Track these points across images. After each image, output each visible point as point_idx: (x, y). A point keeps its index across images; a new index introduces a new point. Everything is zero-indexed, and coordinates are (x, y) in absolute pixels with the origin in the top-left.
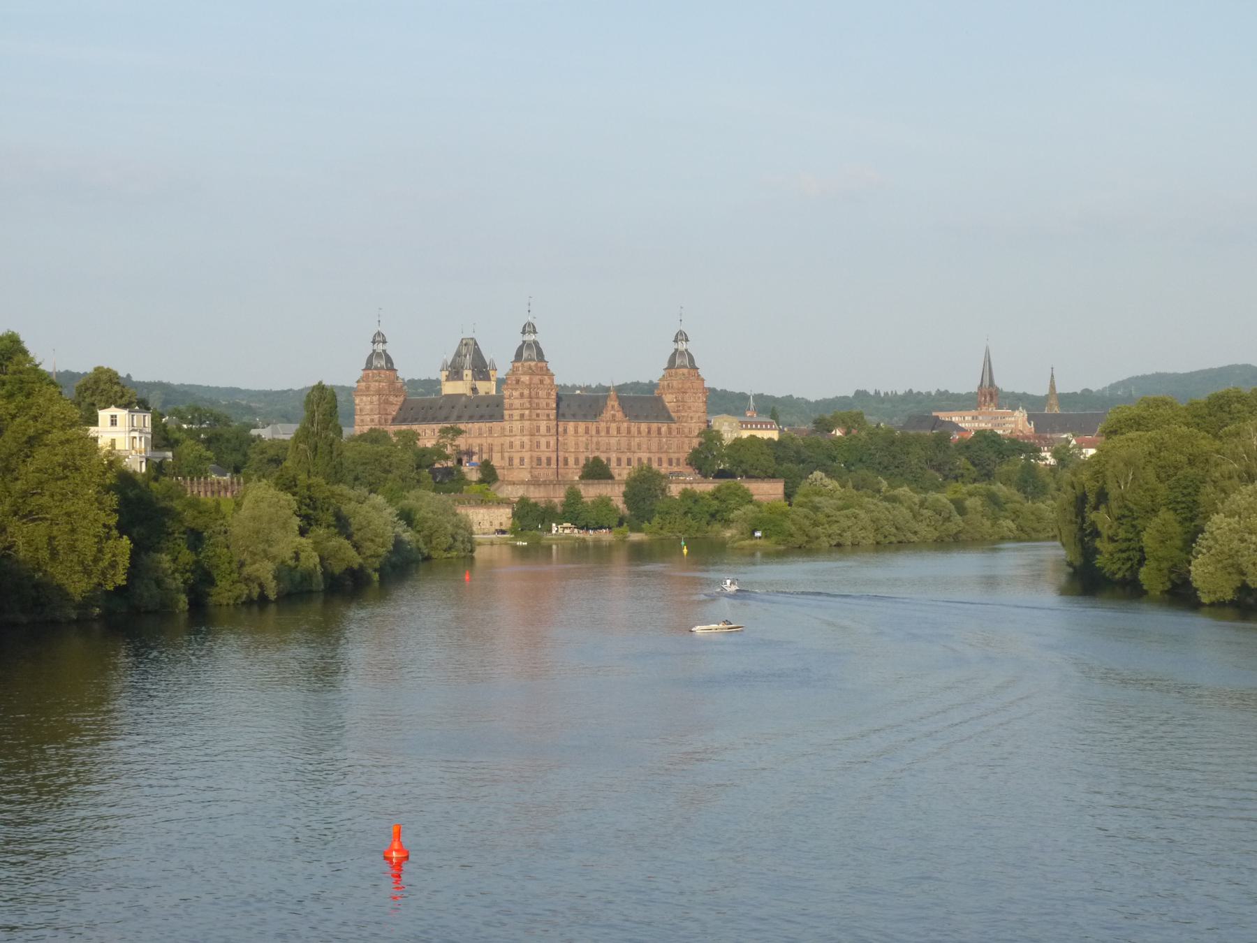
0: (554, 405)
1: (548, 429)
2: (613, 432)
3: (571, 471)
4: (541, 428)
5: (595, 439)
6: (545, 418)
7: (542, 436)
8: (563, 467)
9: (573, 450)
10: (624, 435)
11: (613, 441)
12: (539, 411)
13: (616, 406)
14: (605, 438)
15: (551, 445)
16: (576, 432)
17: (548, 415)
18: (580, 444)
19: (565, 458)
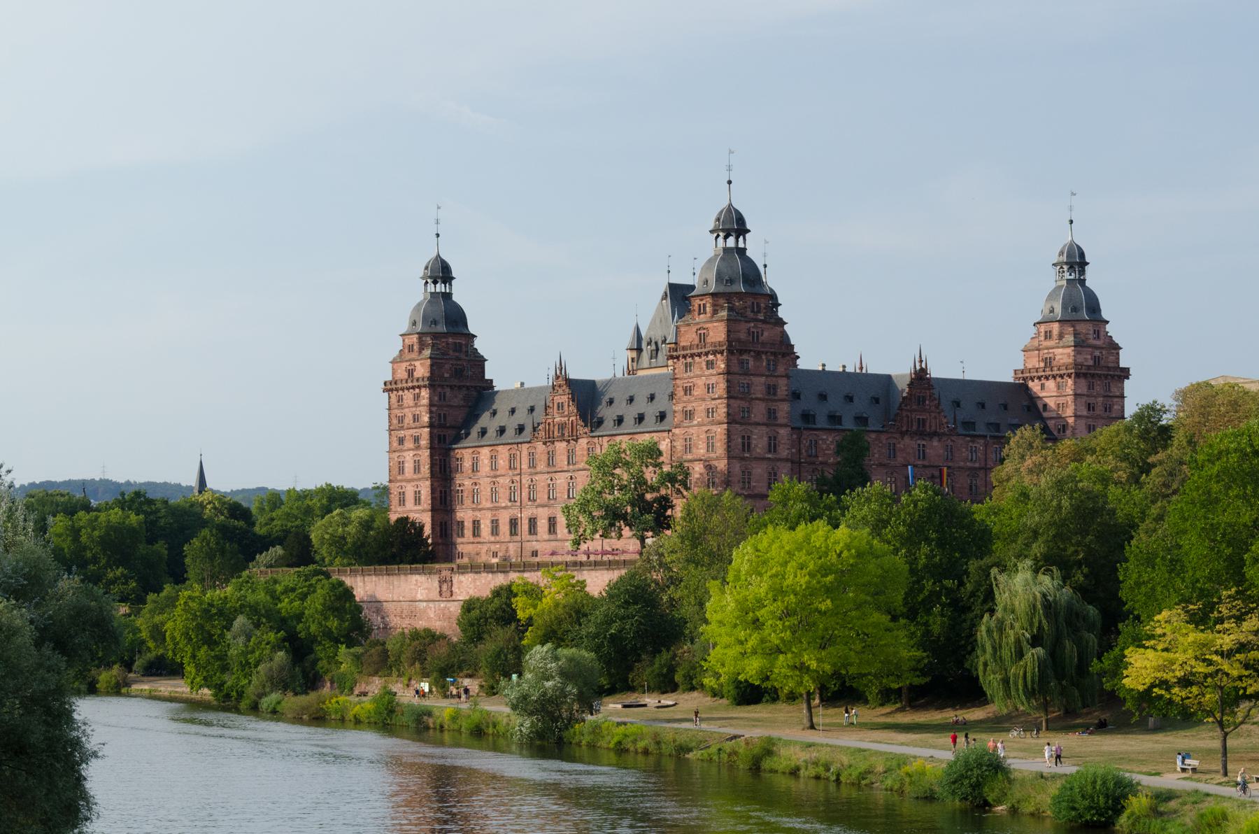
0: (426, 418)
1: (417, 469)
2: (561, 460)
3: (485, 548)
4: (406, 465)
5: (526, 480)
6: (412, 445)
7: (409, 481)
8: (472, 539)
9: (489, 505)
10: (582, 465)
11: (561, 480)
12: (402, 433)
13: (566, 407)
14: (547, 476)
15: (422, 497)
16: (494, 467)
17: (417, 439)
18: (501, 490)
19: (474, 522)
